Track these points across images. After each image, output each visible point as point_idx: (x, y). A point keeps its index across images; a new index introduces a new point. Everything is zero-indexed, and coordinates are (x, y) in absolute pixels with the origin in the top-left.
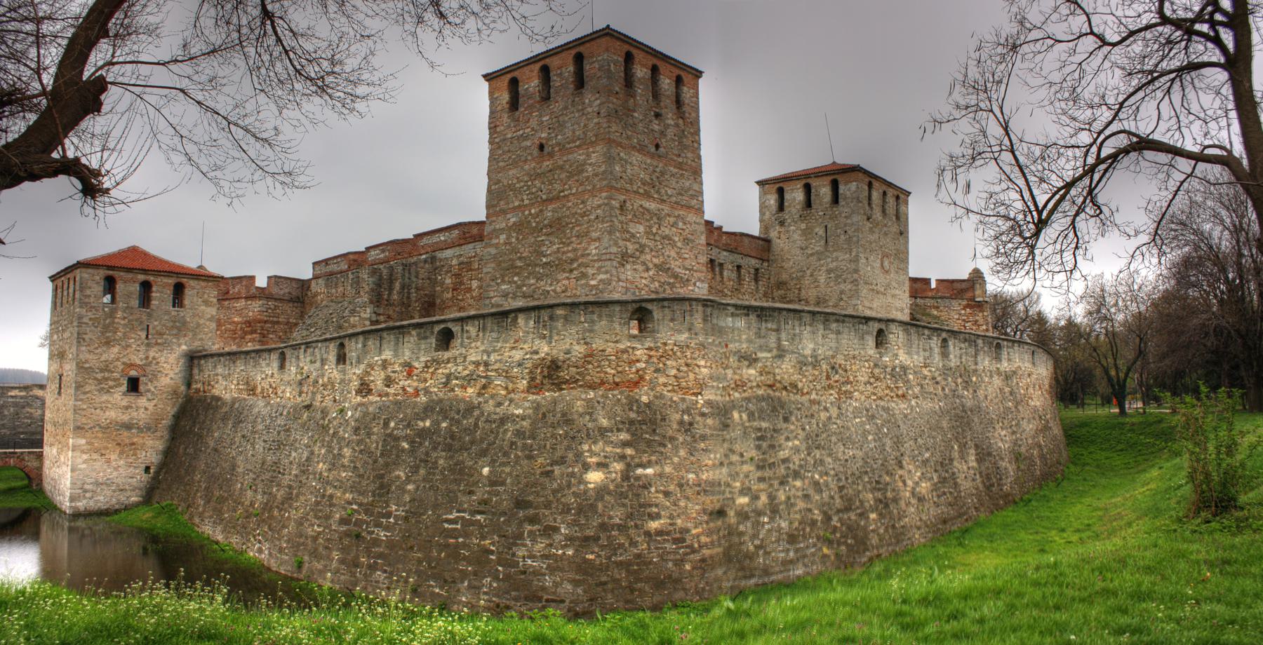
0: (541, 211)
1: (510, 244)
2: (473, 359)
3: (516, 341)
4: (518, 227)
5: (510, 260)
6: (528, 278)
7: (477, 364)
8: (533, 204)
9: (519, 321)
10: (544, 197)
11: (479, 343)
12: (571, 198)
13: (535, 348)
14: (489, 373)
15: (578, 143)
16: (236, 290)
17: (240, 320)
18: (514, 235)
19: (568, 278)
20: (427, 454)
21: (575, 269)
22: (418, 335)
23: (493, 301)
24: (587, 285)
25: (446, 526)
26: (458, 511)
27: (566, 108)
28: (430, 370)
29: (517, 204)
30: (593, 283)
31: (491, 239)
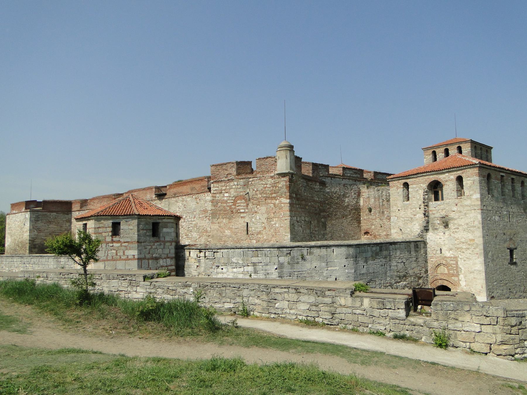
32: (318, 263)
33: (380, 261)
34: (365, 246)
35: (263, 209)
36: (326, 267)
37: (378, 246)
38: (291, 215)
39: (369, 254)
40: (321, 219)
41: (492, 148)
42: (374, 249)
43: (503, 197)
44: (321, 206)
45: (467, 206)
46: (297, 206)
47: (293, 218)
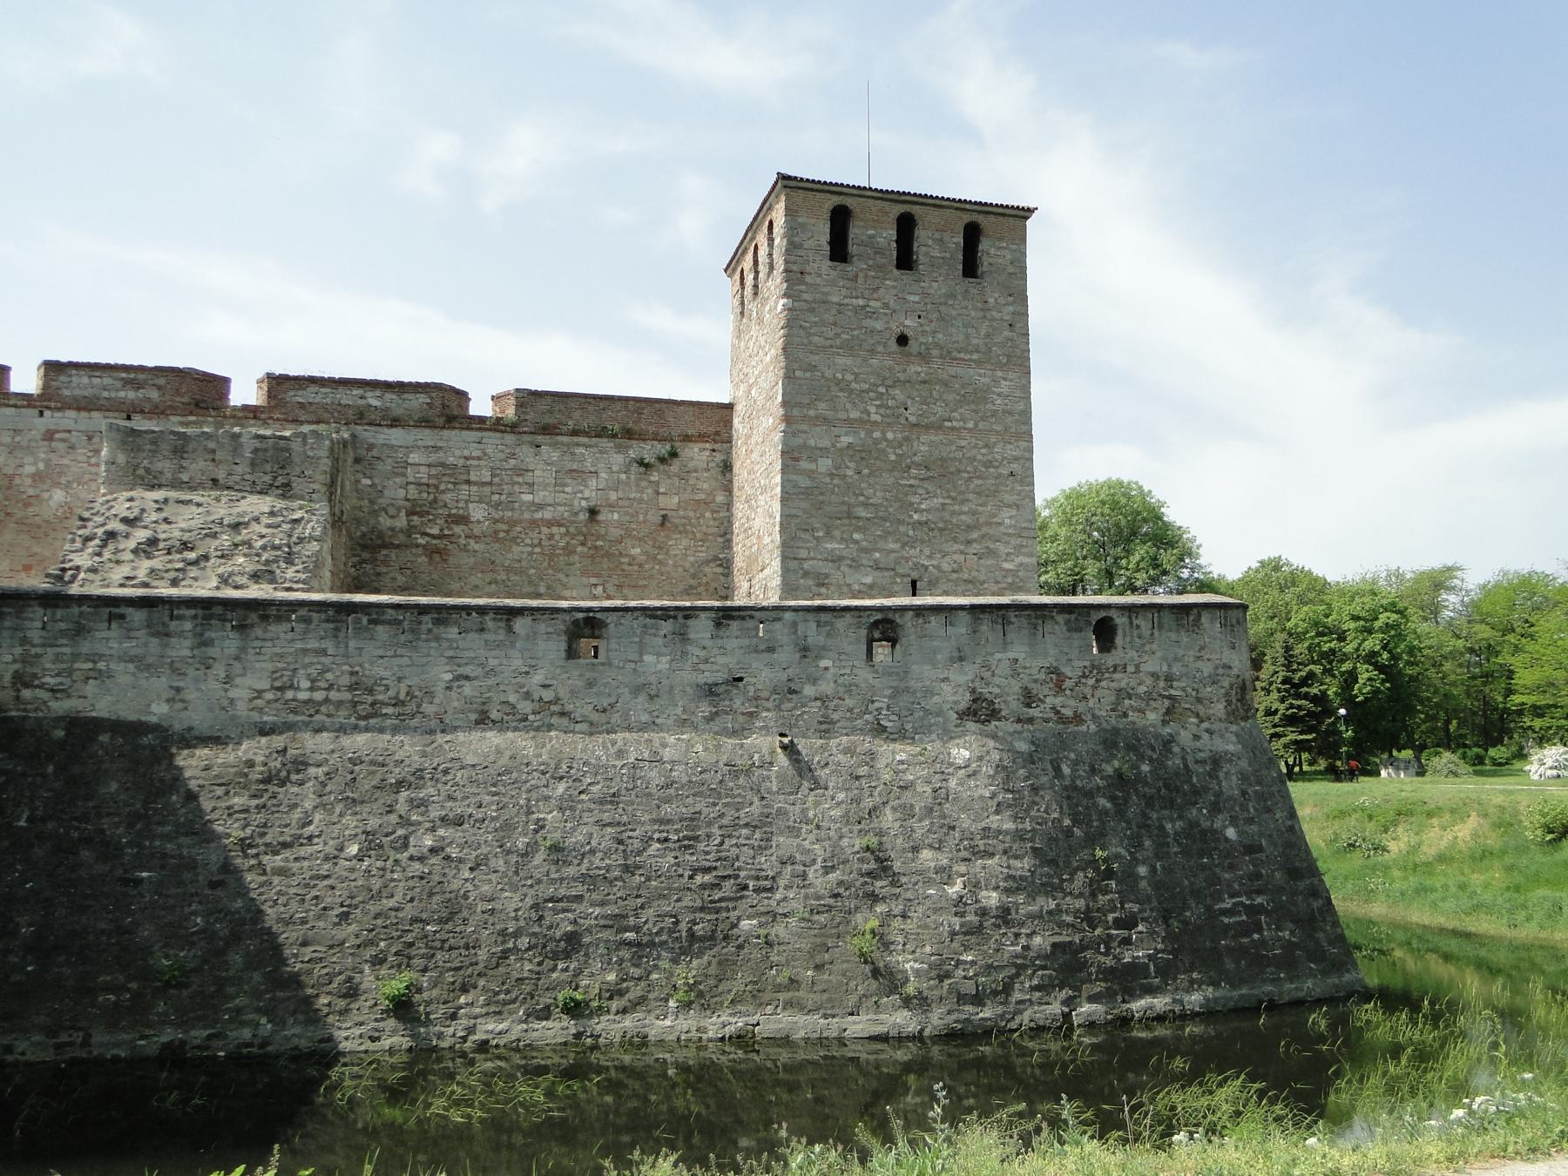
0: (907, 439)
2: (1151, 669)
3: (1202, 648)
4: (861, 454)
5: (843, 503)
7: (1154, 675)
9: (1203, 620)
10: (912, 419)
11: (1155, 646)
12: (965, 433)
13: (1224, 661)
14: (1173, 692)
15: (975, 356)
18: (852, 465)
19: (962, 552)
20: (1145, 815)
21: (975, 540)
22: (1067, 622)
25: (1226, 920)
26: (1232, 896)
28: (1091, 682)
29: (854, 415)
30: (1006, 566)
41: (1029, 211)
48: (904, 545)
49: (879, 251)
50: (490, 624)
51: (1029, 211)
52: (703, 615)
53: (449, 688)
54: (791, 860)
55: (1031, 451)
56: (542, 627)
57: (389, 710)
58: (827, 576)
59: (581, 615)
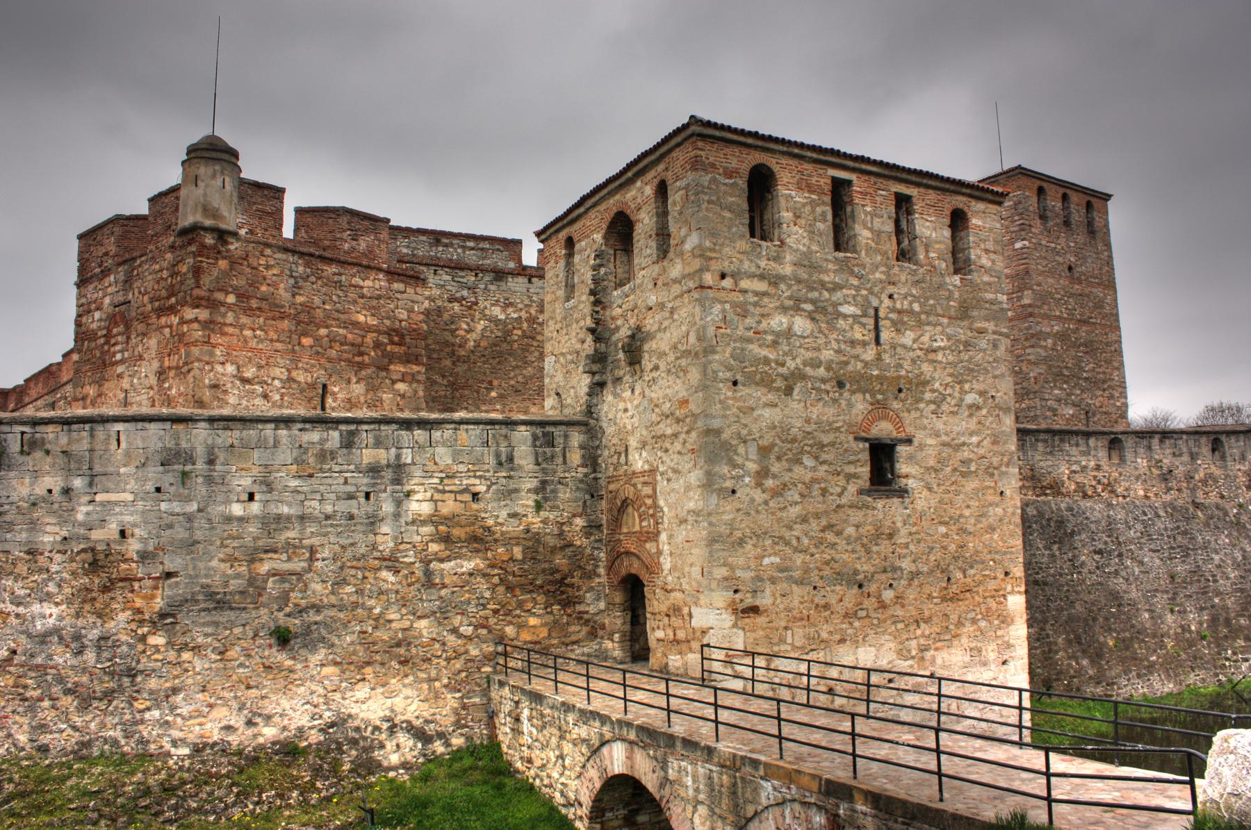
0: (1077, 329)
1: (1057, 350)
4: (1062, 336)
5: (1058, 366)
6: (1074, 387)
8: (1071, 319)
16: (363, 245)
17: (372, 321)
23: (1049, 403)
24: (1114, 404)
27: (1086, 244)
29: (1058, 313)
30: (1118, 404)
31: (1039, 339)
32: (59, 478)
33: (342, 481)
34: (260, 426)
35: (153, 343)
36: (87, 490)
37: (337, 429)
38: (207, 358)
39: (285, 455)
40: (394, 382)
41: (1110, 196)
42: (314, 436)
43: (841, 255)
44: (392, 343)
45: (675, 281)
46: (248, 333)
47: (219, 368)
48: (1082, 391)
49: (1057, 216)
50: (1080, 442)
51: (1110, 196)
52: (1158, 436)
53: (1069, 478)
54: (1219, 566)
55: (1120, 337)
56: (1100, 444)
57: (1048, 491)
58: (1056, 410)
59: (1113, 436)
